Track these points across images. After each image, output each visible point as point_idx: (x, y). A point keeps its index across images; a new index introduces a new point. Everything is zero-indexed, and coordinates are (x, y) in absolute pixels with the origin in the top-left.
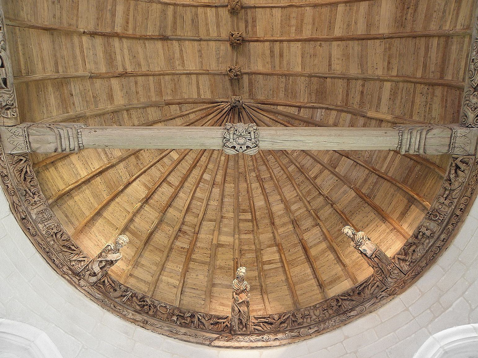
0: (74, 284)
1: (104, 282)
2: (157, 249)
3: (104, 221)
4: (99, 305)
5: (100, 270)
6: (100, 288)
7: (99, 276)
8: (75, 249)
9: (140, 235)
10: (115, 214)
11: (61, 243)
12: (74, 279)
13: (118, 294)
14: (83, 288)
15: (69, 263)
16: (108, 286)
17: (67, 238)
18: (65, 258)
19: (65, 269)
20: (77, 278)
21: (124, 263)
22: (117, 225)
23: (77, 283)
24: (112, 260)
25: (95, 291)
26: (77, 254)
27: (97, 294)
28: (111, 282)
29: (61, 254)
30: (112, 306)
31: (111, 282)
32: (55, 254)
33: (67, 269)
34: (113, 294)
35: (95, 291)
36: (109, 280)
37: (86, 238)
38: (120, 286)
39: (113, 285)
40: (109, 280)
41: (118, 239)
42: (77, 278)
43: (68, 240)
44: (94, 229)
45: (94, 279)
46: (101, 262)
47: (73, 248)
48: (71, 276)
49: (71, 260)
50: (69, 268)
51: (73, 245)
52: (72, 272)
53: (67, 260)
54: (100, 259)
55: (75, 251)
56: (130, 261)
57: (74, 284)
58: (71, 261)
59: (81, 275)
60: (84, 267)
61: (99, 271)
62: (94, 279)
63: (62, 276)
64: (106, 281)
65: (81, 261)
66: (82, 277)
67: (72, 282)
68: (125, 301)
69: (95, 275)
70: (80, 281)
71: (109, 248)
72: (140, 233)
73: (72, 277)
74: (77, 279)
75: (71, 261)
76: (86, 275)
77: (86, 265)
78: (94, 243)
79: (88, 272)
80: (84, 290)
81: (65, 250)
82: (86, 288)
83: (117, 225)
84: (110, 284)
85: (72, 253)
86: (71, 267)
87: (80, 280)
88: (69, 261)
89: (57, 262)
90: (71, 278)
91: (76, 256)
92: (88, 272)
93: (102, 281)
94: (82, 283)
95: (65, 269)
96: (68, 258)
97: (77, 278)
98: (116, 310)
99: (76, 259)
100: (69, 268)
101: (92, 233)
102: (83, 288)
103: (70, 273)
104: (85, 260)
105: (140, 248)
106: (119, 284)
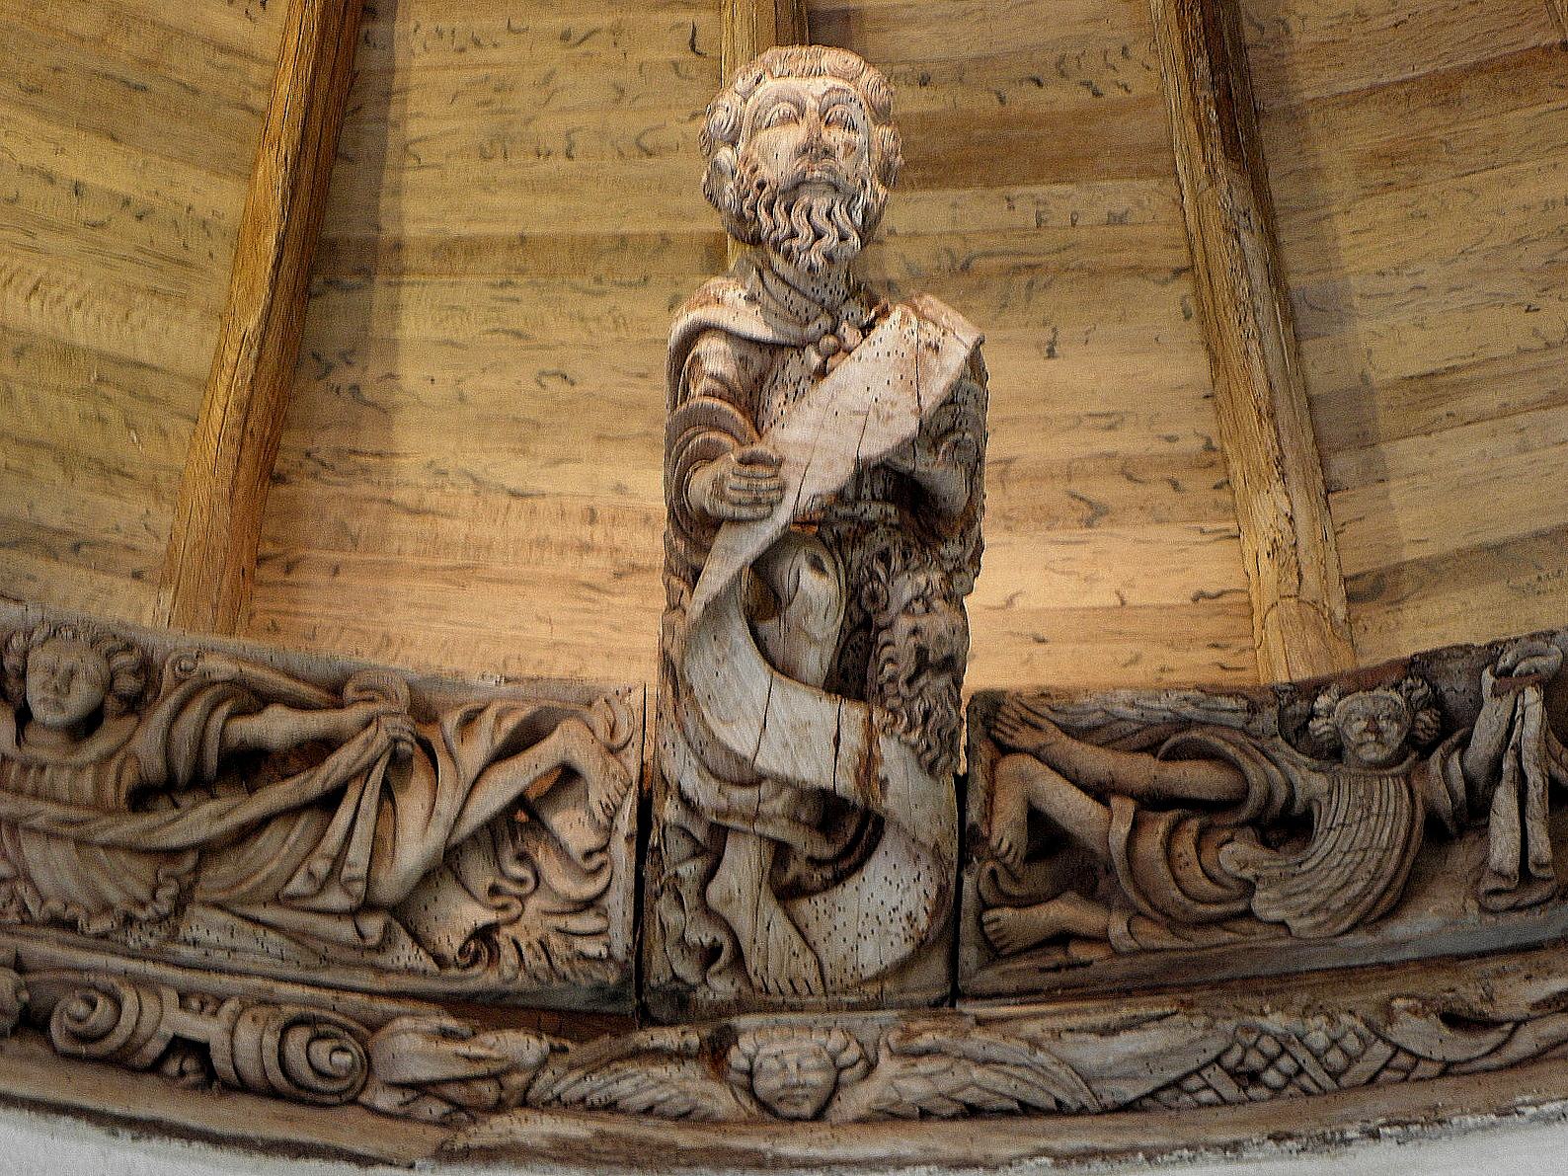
0: (685, 1138)
1: (1040, 824)
2: (1443, 89)
3: (472, 289)
4: (1235, 1147)
5: (855, 712)
6: (1078, 952)
7: (909, 792)
8: (315, 723)
9: (1081, 116)
10: (550, 127)
11: (76, 775)
12: (633, 1084)
13: (1361, 828)
14: (860, 1098)
15: (406, 953)
16: (1151, 844)
17: (91, 665)
18: (298, 937)
19: (415, 1048)
20: (667, 1038)
21: (1154, 532)
22: (681, 215)
23: (722, 1100)
24: (875, 446)
25: (1032, 1028)
26: (398, 763)
27: (1093, 1053)
28: (1141, 770)
29: (206, 927)
30: (1418, 1033)
31: (1141, 770)
32: (139, 983)
33: (446, 1034)
34: (1298, 896)
35: (1032, 1028)
36: (1097, 761)
37: (397, 585)
38: (1297, 732)
39: (1197, 778)
40: (1097, 761)
41: (725, 155)
42: (658, 1054)
43: (127, 684)
44: (420, 449)
45: (882, 906)
46: (763, 596)
47: (277, 726)
48: (571, 1085)
49: (391, 884)
50: (453, 1003)
51: (254, 699)
52: (538, 1031)
53: (345, 930)
54: (718, 574)
55: (321, 747)
56: (1211, 457)
57: (685, 1138)
58: (405, 914)
59: (687, 970)
60: (622, 852)
61: (853, 739)
62: (882, 906)
63: (445, 1155)
64: (1069, 805)
65: (523, 819)
66: (722, 987)
67: (648, 1130)
68: (1541, 846)
69: (843, 828)
70: (737, 1058)
71: (716, 358)
72: (1062, 97)
73: (596, 1086)
74: (680, 1056)
75: (405, 914)
76: (743, 923)
77: (629, 806)
78: (555, 581)
79: (741, 869)
80: (889, 1116)
81: (200, 820)
82: (898, 1080)
83: (681, 215)
84: (1152, 801)
85: (329, 802)
86: (483, 978)
87: (715, 1053)
88: (373, 925)
89: (248, 1044)
90: (585, 1107)
91: (412, 803)
92: (741, 869)
93: (1006, 830)
94: (783, 1051)
95: (415, 1048)
96: (336, 899)
97: (658, 1054)
98: (1525, 1043)
99: (436, 836)
100: (453, 1003)
101: (432, 499)
102: (860, 1098)
103: (521, 1046)
104: (568, 775)
105: (1215, 230)
106: (1268, 719)
